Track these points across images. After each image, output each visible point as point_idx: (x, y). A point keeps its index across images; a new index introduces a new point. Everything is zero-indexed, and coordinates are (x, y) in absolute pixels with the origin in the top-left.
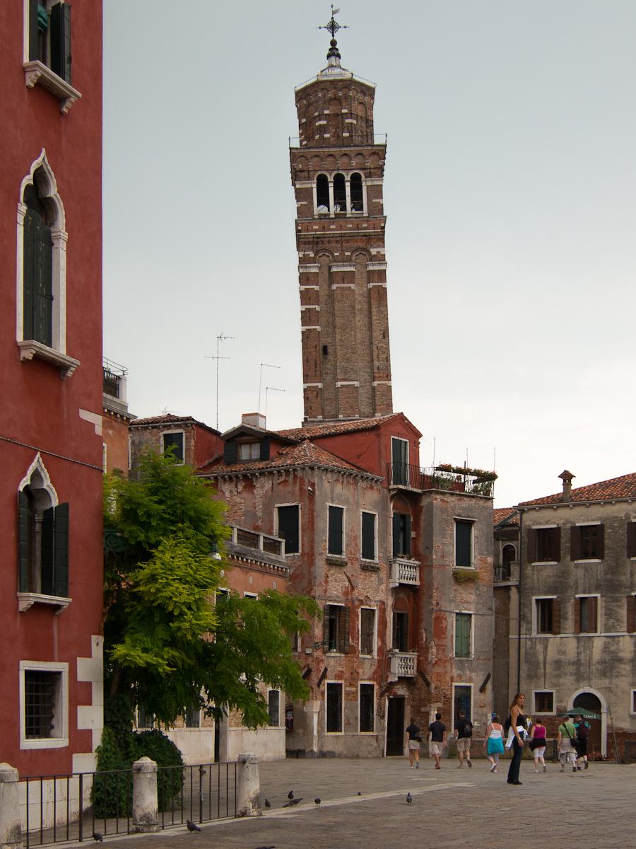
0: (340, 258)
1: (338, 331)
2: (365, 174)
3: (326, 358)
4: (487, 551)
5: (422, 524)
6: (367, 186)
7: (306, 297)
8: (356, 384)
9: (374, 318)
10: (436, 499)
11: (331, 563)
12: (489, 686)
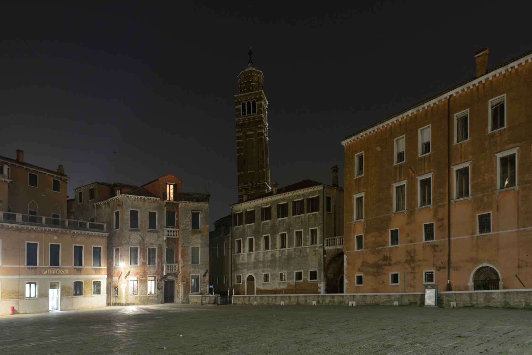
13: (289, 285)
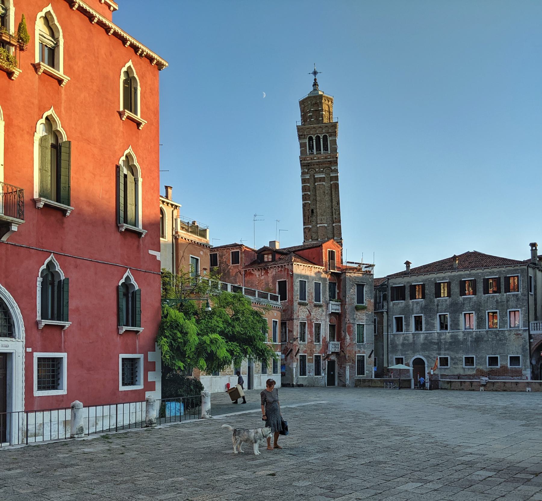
5: (342, 287)
7: (304, 189)
8: (326, 225)
11: (300, 304)
12: (373, 355)
13: (478, 370)
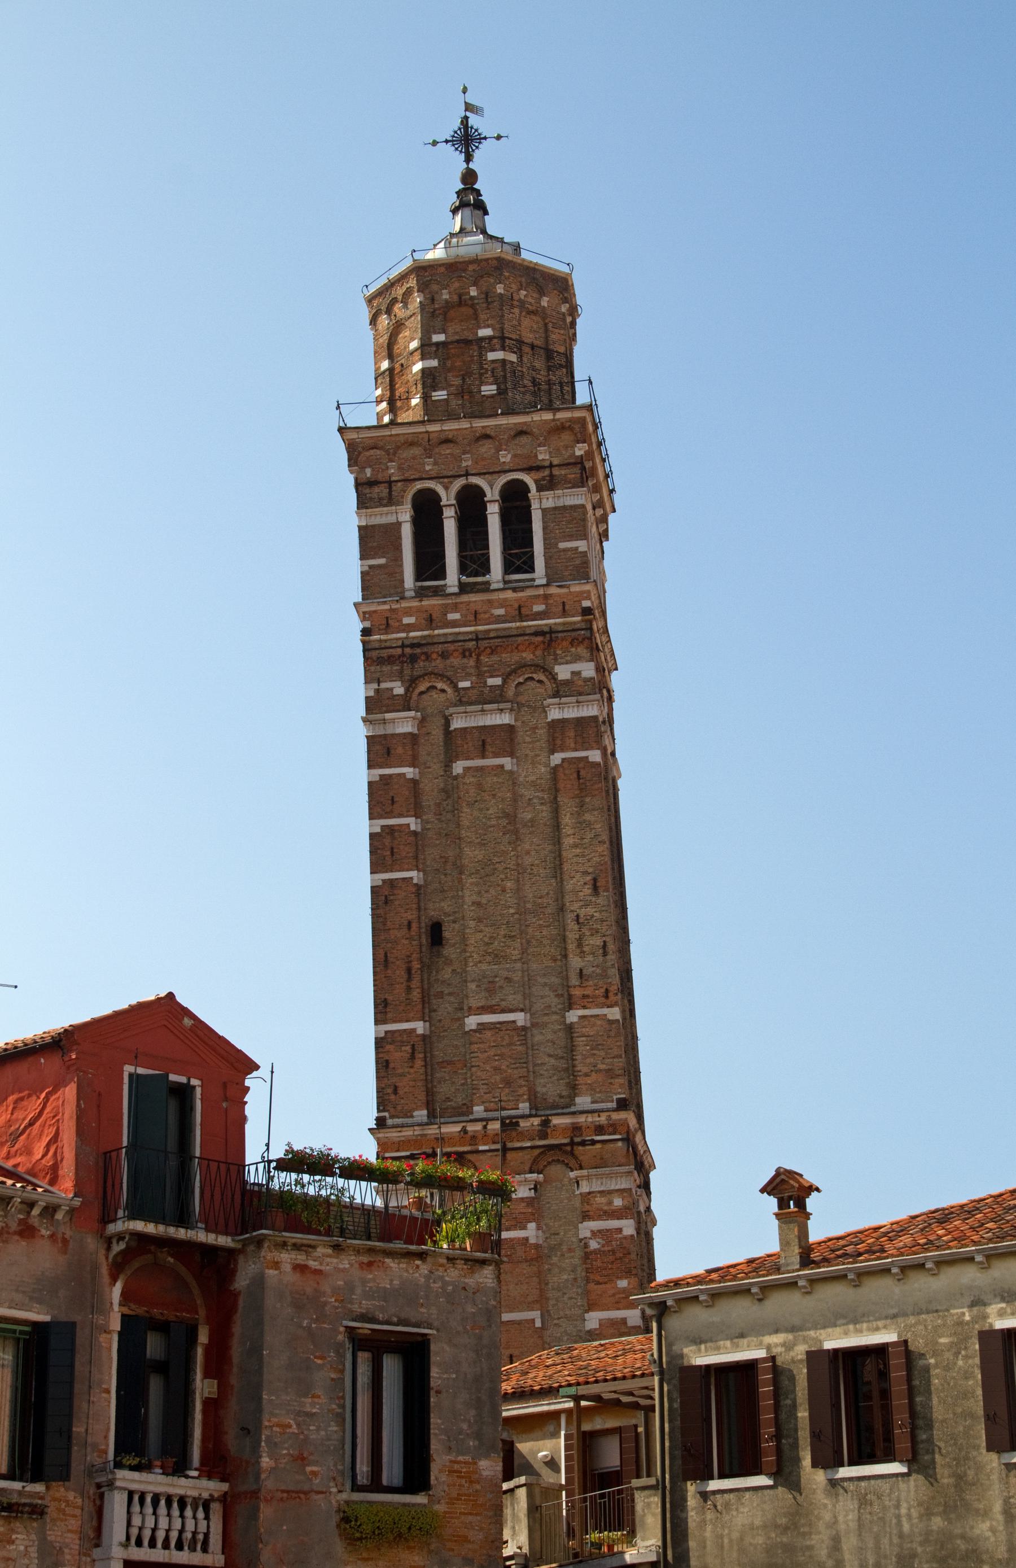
0: (473, 695)
1: (469, 881)
2: (536, 481)
3: (439, 955)
4: (478, 1436)
5: (236, 1351)
6: (545, 511)
7: (381, 798)
8: (520, 1018)
9: (568, 841)
10: (276, 1265)
